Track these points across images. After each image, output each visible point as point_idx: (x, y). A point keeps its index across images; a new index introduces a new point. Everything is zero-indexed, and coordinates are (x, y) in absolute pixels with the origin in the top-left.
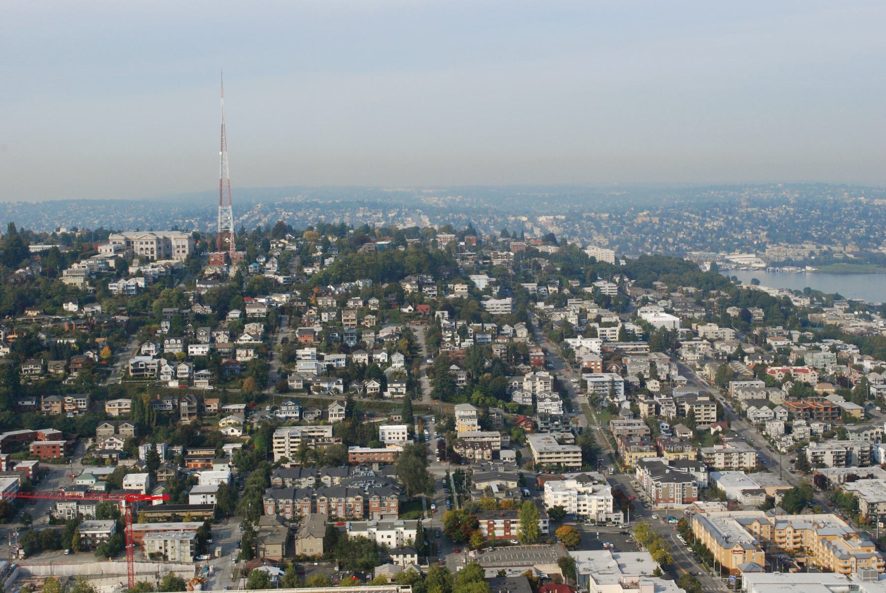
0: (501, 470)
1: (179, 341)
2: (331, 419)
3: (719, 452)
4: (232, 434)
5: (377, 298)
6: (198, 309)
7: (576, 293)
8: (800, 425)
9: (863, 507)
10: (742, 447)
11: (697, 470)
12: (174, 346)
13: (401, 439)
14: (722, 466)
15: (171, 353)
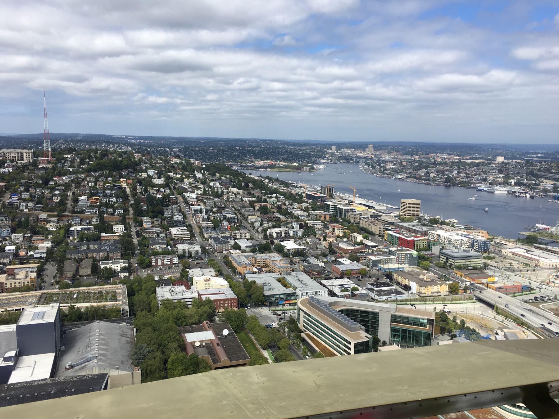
0: (160, 241)
1: (28, 193)
2: (93, 223)
3: (238, 233)
4: (52, 230)
5: (111, 177)
6: (36, 180)
7: (188, 177)
8: (265, 223)
9: (285, 251)
10: (246, 231)
11: (231, 239)
12: (26, 195)
13: (122, 230)
14: (239, 238)
15: (25, 198)
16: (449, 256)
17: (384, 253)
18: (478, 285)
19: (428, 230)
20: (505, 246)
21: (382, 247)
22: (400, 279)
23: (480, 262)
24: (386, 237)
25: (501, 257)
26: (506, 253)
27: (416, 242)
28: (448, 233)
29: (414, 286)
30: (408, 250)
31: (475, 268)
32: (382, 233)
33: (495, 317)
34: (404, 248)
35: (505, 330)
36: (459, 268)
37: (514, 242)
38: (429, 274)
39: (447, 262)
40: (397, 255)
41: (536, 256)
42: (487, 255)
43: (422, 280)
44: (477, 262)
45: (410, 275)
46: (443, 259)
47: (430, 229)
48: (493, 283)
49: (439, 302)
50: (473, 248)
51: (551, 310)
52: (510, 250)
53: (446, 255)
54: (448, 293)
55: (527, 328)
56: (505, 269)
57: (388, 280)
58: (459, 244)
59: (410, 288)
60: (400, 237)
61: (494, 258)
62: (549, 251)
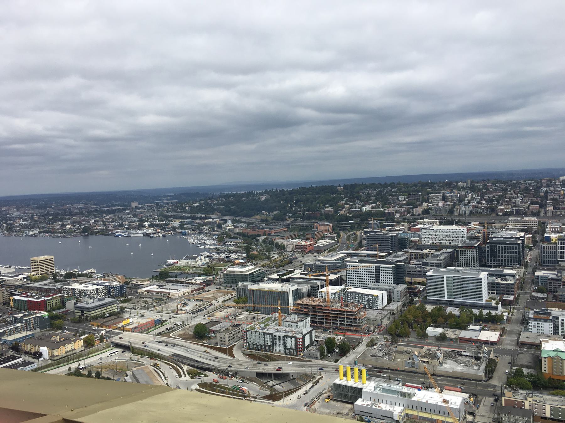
16: (83, 308)
17: (9, 323)
18: (115, 331)
19: (62, 285)
20: (141, 286)
21: (7, 316)
22: (29, 348)
23: (116, 307)
24: (12, 303)
25: (137, 297)
26: (141, 292)
27: (47, 302)
28: (83, 285)
29: (44, 350)
30: (37, 313)
31: (111, 314)
32: (6, 300)
33: (131, 358)
34: (32, 312)
35: (134, 369)
36: (96, 318)
37: (149, 280)
38: (64, 334)
39: (83, 315)
40: (24, 321)
41: (167, 289)
42: (124, 298)
43: (54, 342)
44: (113, 308)
45: (42, 341)
46: (78, 313)
47: (64, 285)
48: (129, 324)
49: (75, 361)
50: (110, 295)
51: (180, 336)
52: (144, 289)
53: (81, 308)
54: (83, 348)
55: (159, 359)
56: (140, 308)
57: (15, 352)
58: (95, 294)
59: (41, 355)
60: (28, 300)
61: (131, 299)
62: (178, 282)
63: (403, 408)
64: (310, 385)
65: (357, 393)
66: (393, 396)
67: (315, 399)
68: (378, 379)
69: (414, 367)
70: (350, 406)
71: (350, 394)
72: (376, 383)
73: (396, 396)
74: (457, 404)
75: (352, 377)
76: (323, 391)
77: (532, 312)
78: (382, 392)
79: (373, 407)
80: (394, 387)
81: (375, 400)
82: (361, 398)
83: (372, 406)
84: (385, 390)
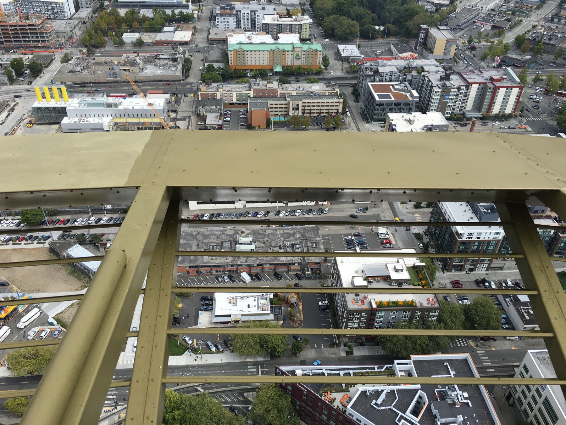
63: (111, 118)
64: (5, 113)
65: (62, 112)
66: (100, 108)
67: (15, 127)
68: (80, 95)
69: (116, 77)
70: (57, 126)
71: (53, 114)
72: (80, 99)
73: (103, 108)
74: (160, 105)
75: (52, 97)
76: (22, 117)
77: (218, 7)
78: (88, 107)
79: (81, 122)
80: (99, 99)
81: (81, 116)
82: (67, 116)
83: (80, 122)
84: (90, 104)
